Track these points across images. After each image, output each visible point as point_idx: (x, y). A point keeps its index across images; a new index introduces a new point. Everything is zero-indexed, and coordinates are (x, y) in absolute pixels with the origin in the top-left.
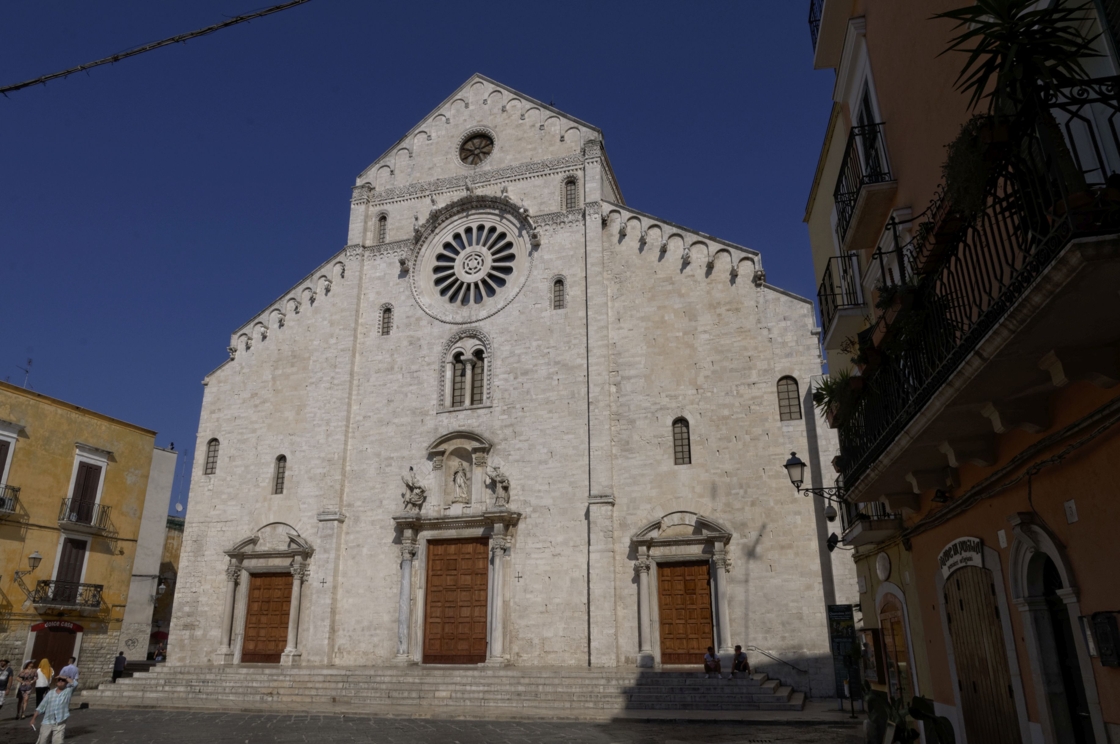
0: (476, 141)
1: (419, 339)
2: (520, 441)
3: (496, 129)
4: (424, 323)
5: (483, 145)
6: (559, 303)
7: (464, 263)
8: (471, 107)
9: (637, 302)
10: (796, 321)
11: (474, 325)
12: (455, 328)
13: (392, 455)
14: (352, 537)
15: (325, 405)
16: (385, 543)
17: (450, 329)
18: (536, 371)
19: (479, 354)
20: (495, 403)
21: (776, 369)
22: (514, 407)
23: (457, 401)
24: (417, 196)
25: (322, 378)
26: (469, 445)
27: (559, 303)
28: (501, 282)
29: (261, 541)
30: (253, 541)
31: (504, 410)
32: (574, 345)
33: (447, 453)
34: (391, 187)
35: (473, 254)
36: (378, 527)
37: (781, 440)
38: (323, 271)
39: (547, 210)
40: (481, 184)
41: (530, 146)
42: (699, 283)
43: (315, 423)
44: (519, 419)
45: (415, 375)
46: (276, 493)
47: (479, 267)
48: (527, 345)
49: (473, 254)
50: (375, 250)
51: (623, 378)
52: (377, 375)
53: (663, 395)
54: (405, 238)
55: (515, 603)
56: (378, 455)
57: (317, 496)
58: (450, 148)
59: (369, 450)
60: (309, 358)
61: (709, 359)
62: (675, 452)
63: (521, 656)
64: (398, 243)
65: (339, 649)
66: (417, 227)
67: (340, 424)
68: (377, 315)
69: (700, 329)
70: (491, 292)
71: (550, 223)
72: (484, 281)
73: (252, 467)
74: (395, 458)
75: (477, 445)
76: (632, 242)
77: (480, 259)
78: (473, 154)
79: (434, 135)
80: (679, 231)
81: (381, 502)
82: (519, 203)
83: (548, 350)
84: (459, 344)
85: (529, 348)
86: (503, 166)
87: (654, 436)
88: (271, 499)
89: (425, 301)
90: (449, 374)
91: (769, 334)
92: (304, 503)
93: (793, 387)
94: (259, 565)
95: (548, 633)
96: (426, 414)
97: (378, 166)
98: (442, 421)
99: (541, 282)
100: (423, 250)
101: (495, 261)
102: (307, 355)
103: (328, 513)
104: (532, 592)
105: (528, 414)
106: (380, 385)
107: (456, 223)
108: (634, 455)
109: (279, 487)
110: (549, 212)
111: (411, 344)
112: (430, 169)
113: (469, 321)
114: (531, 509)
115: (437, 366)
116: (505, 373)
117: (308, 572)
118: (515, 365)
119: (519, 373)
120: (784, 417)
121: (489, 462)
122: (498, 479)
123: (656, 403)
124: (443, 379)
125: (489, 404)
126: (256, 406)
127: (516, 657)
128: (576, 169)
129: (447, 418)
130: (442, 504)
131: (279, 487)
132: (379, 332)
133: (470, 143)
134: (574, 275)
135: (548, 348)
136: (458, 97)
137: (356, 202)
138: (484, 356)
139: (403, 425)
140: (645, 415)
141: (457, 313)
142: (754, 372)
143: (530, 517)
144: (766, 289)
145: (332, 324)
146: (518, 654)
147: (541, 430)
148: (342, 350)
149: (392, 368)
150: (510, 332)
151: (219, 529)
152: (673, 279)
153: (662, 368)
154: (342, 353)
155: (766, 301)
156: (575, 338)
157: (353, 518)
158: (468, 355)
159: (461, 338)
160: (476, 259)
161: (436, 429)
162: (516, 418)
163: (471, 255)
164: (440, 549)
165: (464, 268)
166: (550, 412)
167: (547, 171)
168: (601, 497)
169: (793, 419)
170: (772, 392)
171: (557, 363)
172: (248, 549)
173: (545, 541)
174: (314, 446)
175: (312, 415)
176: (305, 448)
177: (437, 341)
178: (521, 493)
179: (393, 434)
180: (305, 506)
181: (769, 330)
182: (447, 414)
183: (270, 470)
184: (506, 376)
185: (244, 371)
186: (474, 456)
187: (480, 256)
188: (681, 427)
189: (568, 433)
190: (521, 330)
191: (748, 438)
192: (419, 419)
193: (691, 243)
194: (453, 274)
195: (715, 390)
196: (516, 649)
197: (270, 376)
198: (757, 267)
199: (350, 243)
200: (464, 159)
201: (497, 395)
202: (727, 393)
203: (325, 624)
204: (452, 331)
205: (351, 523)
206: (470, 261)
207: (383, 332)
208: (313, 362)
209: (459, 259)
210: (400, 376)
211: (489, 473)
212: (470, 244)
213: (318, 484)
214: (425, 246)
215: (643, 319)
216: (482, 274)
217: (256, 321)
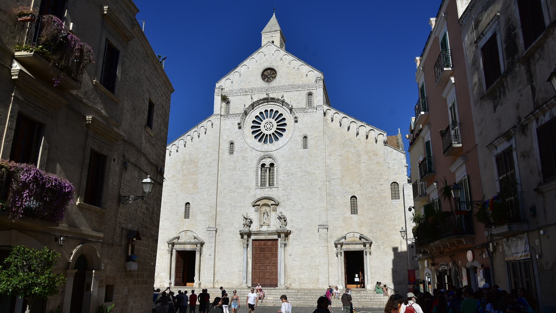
0: (269, 71)
2: (290, 202)
3: (278, 68)
4: (248, 150)
5: (271, 74)
6: (305, 146)
7: (265, 125)
8: (266, 56)
9: (337, 148)
10: (399, 161)
11: (270, 153)
12: (262, 154)
13: (237, 205)
14: (221, 237)
15: (206, 182)
16: (235, 240)
17: (260, 154)
18: (296, 174)
19: (272, 165)
21: (391, 179)
22: (288, 188)
23: (263, 185)
24: (244, 94)
25: (204, 171)
28: (281, 135)
29: (180, 238)
30: (178, 238)
31: (283, 189)
32: (312, 164)
33: (260, 205)
34: (232, 89)
35: (269, 122)
36: (231, 234)
37: (391, 207)
38: (203, 124)
39: (300, 106)
40: (272, 92)
41: (293, 77)
42: (362, 142)
43: (202, 190)
44: (289, 193)
45: (245, 172)
46: (186, 218)
47: (271, 128)
48: (293, 163)
49: (269, 122)
50: (226, 117)
51: (331, 179)
52: (229, 171)
53: (347, 187)
54: (239, 113)
55: (289, 265)
56: (231, 205)
57: (205, 220)
58: (258, 74)
59: (226, 202)
60: (198, 162)
61: (365, 174)
62: (351, 209)
63: (291, 285)
64: (236, 115)
65: (217, 281)
66: (245, 109)
67: (214, 191)
68: (227, 146)
69: (362, 161)
70: (277, 139)
71: (302, 112)
72: (273, 134)
73: (175, 207)
74: (238, 206)
75: (273, 203)
76: (336, 123)
77: (271, 124)
78: (268, 77)
79: (250, 67)
80: (355, 120)
81: (233, 224)
82: (289, 103)
83: (301, 166)
84: (263, 160)
85: (293, 164)
86: (281, 84)
87: (343, 203)
88: (184, 221)
89: (248, 141)
91: (389, 165)
92: (199, 223)
93: (396, 186)
94: (180, 247)
95: (302, 276)
96: (251, 189)
97: (225, 79)
98: (258, 192)
99: (298, 137)
100: (247, 118)
101: (278, 126)
102: (197, 161)
103: (211, 228)
104: (295, 261)
105: (293, 191)
106: (230, 176)
107: (261, 108)
108: (335, 210)
109: (187, 215)
110: (301, 107)
111: (243, 159)
112: (249, 82)
113: (268, 151)
114: (295, 229)
115: (255, 170)
116: (283, 174)
117: (203, 251)
118: (288, 171)
119: (289, 175)
120: (393, 198)
121: (278, 209)
122: (282, 217)
123: (344, 190)
124: (257, 175)
125: (277, 186)
126: (175, 181)
127: (289, 285)
128: (313, 89)
129: (259, 191)
130: (259, 225)
131: (187, 215)
132: (228, 153)
133: (266, 72)
134: (311, 135)
135: (301, 165)
136: (260, 51)
137: (217, 95)
138: (274, 166)
139: (241, 193)
140: (340, 194)
141: (262, 147)
142: (382, 180)
143: (294, 232)
144: (388, 147)
145: (208, 148)
146: (290, 284)
147: (298, 198)
148: (214, 160)
149: (235, 169)
150: (285, 157)
151: (161, 232)
152: (352, 140)
153: (347, 176)
154: (214, 161)
155: (387, 152)
156: (312, 162)
157: (220, 230)
158: (268, 165)
159: (264, 158)
160: (270, 124)
161: (255, 196)
162: (288, 193)
163: (268, 122)
164: (257, 242)
165: (265, 128)
166: (302, 191)
167: (300, 89)
168: (323, 226)
169: (396, 199)
170: (389, 188)
171: (305, 171)
172: (175, 241)
173: (300, 242)
174: (202, 200)
175: (201, 186)
176: (198, 200)
177: (254, 159)
178: (291, 222)
179: (236, 196)
180: (199, 224)
181: (389, 163)
184: (284, 175)
185: (168, 165)
187: (272, 123)
188: (354, 199)
189: (309, 200)
190: (290, 157)
191: (379, 205)
192: (248, 191)
193: (359, 126)
194: (260, 130)
195: (367, 186)
196: (289, 282)
197: (181, 168)
199: (215, 113)
200: (263, 79)
201: (280, 183)
202: (372, 187)
203: (212, 271)
204: (261, 155)
206: (267, 125)
207: (230, 153)
208: (200, 164)
209: (263, 123)
210: (239, 172)
211: (278, 214)
212: (267, 118)
213: (205, 215)
214: (248, 116)
215: (340, 156)
216: (273, 131)
217: (173, 144)
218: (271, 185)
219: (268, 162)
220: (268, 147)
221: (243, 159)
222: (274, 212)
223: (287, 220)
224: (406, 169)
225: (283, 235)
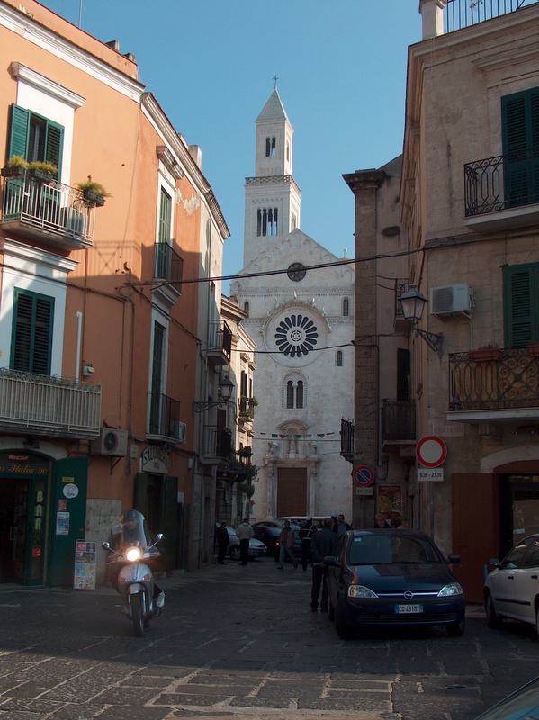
19: (300, 383)
23: (290, 405)
70: (306, 352)
90: (286, 391)
201: (310, 404)
209: (289, 332)
218: (300, 405)
219: (295, 380)
220: (296, 361)
225: (313, 464)
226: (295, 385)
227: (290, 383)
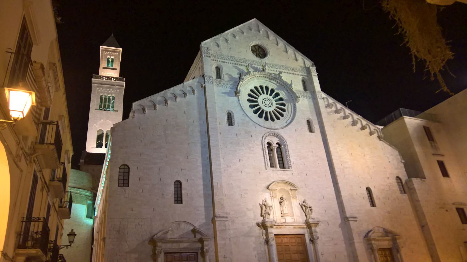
1: (250, 132)
11: (276, 131)
17: (265, 131)
20: (293, 169)
26: (288, 188)
27: (311, 130)
92: (198, 210)
111: (246, 133)
182: (272, 171)
183: (171, 189)
186: (290, 193)
198: (379, 133)
201: (292, 165)
205: (230, 224)
206: (267, 101)
219: (275, 141)
221: (246, 133)
222: (295, 200)
223: (313, 211)
224: (402, 165)
226: (275, 146)
227: (269, 144)
